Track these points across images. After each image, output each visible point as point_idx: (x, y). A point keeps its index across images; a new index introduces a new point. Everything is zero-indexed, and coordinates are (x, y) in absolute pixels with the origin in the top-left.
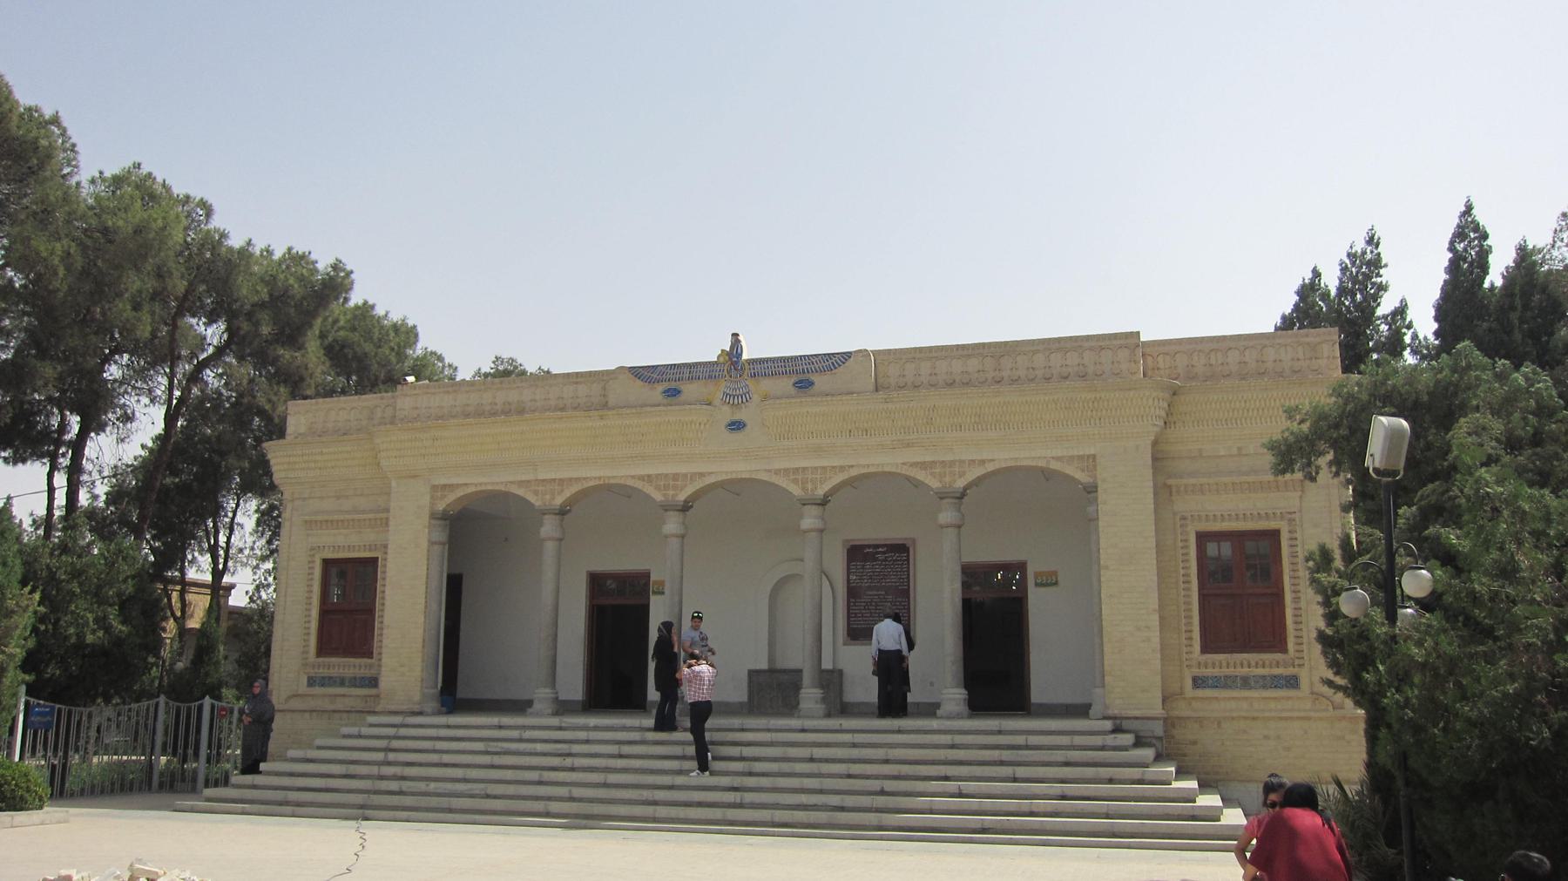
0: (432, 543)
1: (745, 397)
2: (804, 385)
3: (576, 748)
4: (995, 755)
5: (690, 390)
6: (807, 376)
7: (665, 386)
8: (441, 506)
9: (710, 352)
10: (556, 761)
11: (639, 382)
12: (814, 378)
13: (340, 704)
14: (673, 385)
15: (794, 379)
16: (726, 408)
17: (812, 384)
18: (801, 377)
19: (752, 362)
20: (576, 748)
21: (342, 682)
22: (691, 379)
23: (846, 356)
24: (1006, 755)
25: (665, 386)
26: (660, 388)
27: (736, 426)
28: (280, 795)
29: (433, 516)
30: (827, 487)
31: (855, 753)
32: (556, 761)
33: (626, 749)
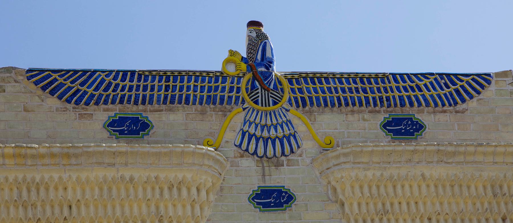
2: (404, 128)
5: (166, 120)
6: (408, 111)
7: (116, 110)
9: (208, 47)
11: (53, 102)
14: (131, 110)
15: (382, 117)
16: (248, 163)
17: (419, 127)
18: (399, 112)
19: (294, 78)
22: (170, 101)
23: (482, 81)
25: (116, 110)
26: (102, 115)
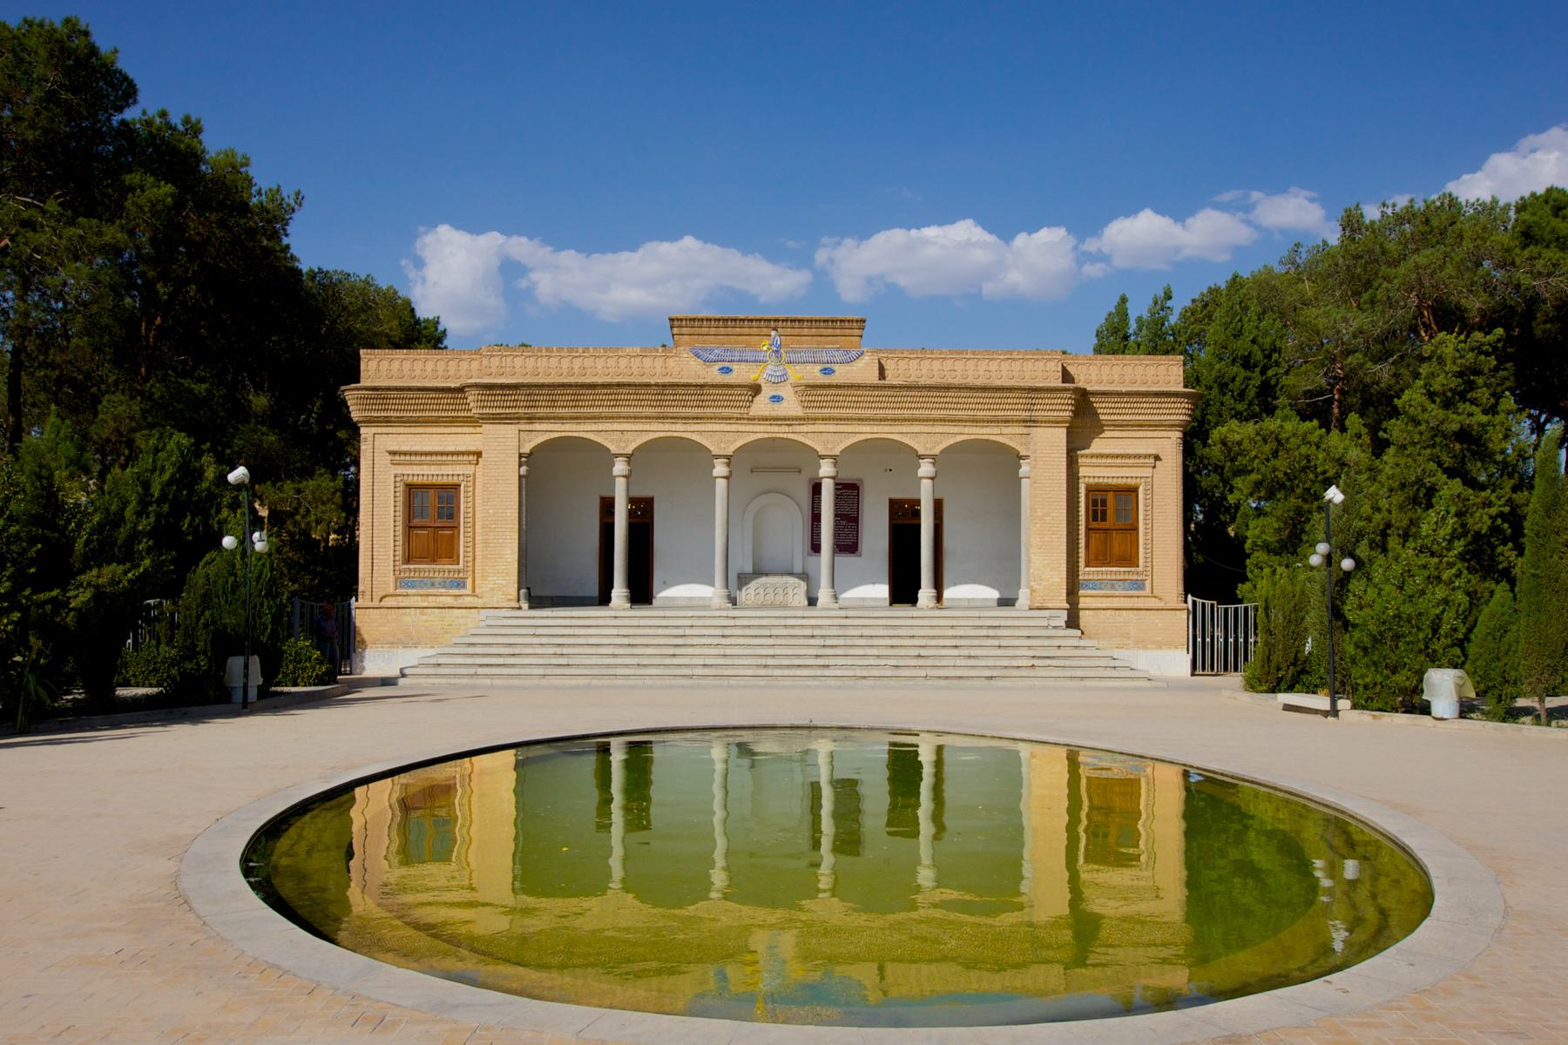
0: (520, 477)
1: (783, 379)
3: (688, 632)
4: (984, 632)
7: (721, 365)
8: (526, 449)
10: (680, 641)
12: (836, 367)
13: (431, 601)
20: (688, 632)
21: (433, 585)
24: (992, 632)
25: (721, 365)
27: (776, 399)
28: (472, 671)
29: (521, 456)
30: (843, 446)
31: (892, 632)
32: (680, 641)
33: (727, 632)
